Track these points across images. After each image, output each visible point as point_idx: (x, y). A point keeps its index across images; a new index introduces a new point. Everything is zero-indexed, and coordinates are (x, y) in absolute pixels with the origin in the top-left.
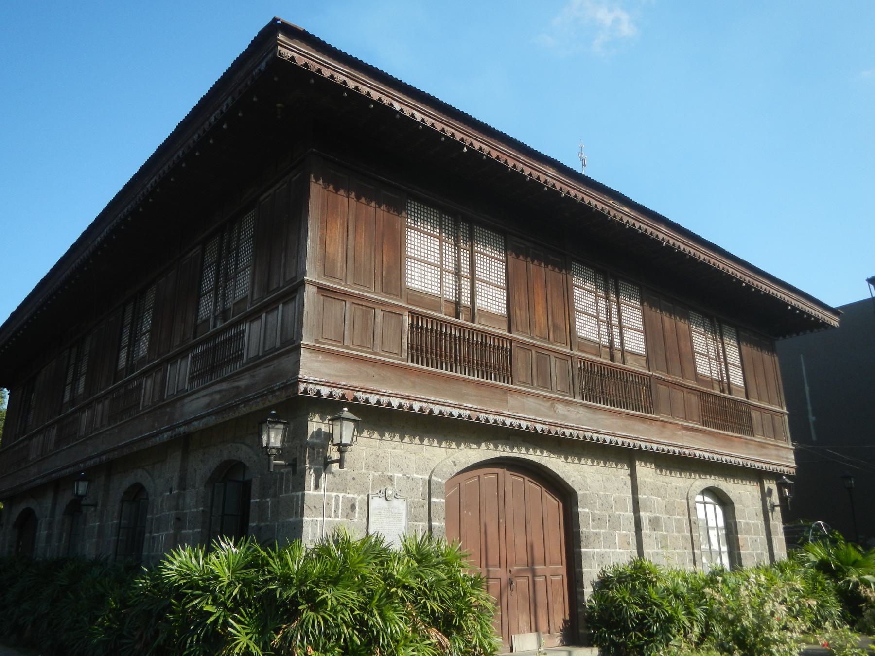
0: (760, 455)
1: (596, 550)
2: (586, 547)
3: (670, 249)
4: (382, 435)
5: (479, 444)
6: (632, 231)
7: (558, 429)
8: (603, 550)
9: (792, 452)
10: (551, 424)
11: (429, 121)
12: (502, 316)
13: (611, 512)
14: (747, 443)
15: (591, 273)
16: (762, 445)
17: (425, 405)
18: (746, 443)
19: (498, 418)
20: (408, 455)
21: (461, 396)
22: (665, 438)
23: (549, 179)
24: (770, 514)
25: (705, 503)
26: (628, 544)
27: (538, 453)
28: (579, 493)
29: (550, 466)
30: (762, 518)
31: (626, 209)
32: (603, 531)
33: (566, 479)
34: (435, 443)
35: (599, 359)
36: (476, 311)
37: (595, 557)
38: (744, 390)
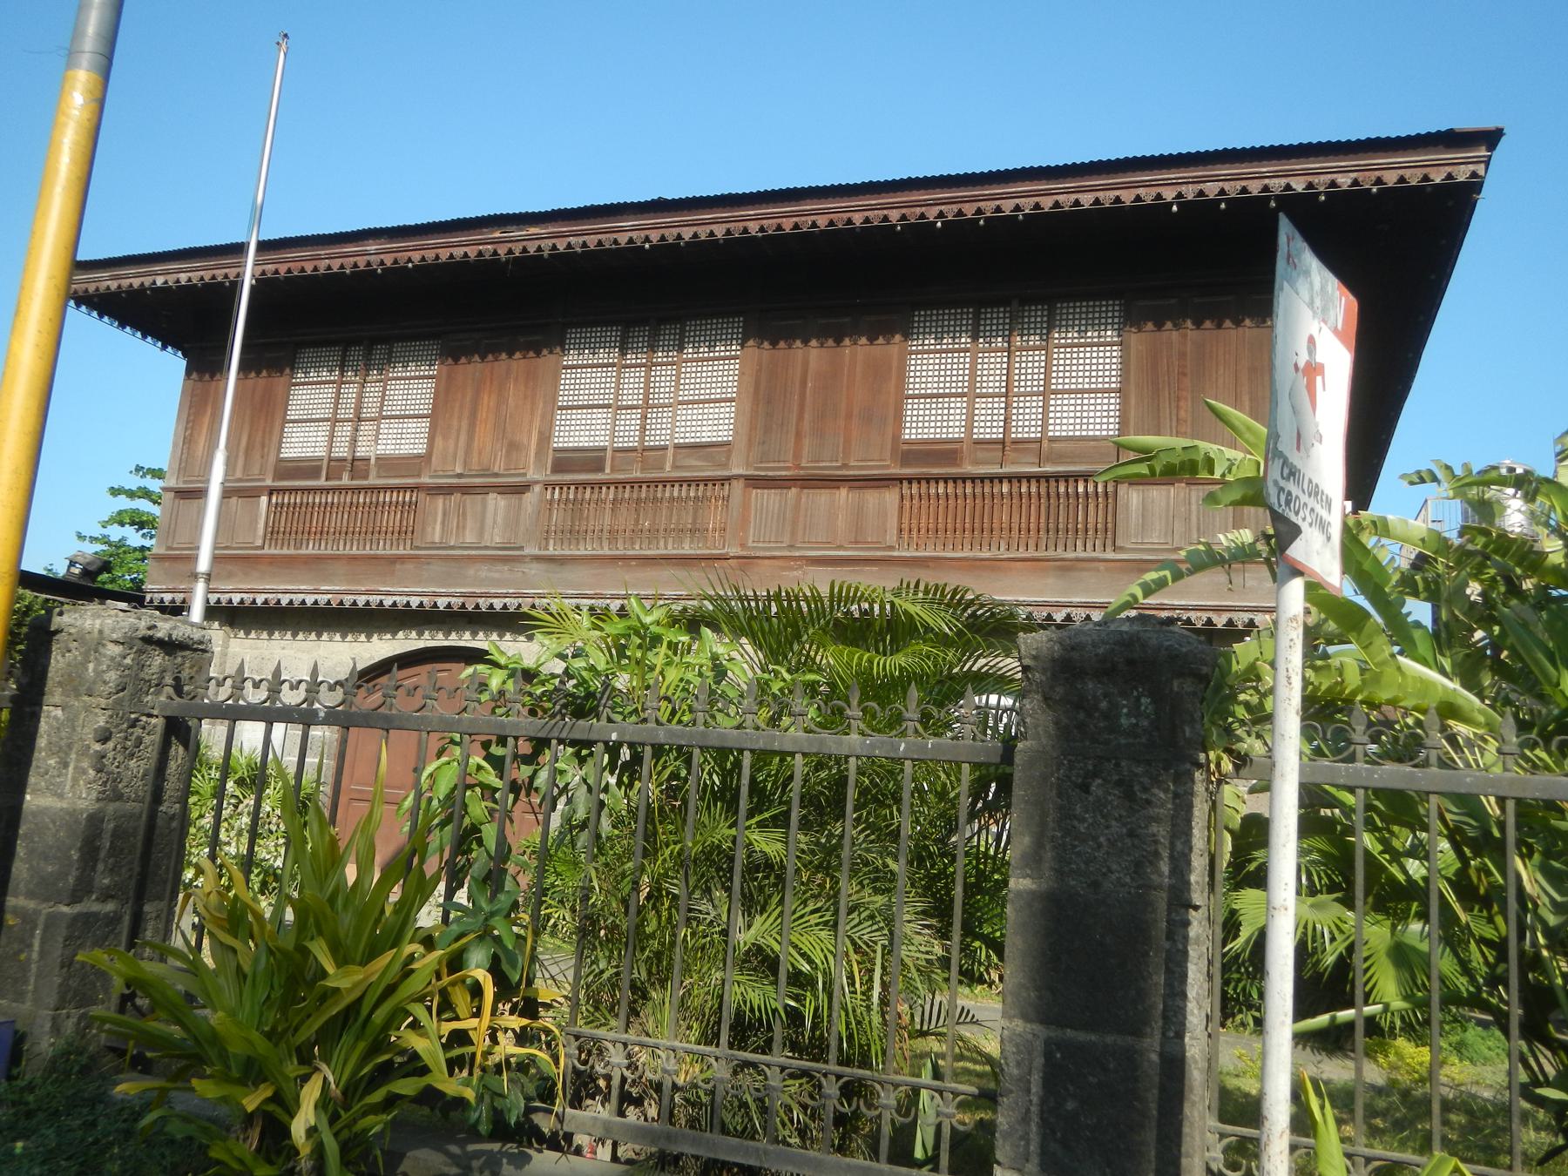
4: (271, 634)
5: (394, 634)
7: (481, 601)
10: (463, 595)
11: (195, 276)
12: (418, 456)
14: (1066, 568)
15: (615, 333)
17: (270, 596)
19: (371, 598)
20: (299, 655)
21: (326, 580)
23: (372, 258)
31: (533, 230)
34: (338, 637)
36: (373, 461)
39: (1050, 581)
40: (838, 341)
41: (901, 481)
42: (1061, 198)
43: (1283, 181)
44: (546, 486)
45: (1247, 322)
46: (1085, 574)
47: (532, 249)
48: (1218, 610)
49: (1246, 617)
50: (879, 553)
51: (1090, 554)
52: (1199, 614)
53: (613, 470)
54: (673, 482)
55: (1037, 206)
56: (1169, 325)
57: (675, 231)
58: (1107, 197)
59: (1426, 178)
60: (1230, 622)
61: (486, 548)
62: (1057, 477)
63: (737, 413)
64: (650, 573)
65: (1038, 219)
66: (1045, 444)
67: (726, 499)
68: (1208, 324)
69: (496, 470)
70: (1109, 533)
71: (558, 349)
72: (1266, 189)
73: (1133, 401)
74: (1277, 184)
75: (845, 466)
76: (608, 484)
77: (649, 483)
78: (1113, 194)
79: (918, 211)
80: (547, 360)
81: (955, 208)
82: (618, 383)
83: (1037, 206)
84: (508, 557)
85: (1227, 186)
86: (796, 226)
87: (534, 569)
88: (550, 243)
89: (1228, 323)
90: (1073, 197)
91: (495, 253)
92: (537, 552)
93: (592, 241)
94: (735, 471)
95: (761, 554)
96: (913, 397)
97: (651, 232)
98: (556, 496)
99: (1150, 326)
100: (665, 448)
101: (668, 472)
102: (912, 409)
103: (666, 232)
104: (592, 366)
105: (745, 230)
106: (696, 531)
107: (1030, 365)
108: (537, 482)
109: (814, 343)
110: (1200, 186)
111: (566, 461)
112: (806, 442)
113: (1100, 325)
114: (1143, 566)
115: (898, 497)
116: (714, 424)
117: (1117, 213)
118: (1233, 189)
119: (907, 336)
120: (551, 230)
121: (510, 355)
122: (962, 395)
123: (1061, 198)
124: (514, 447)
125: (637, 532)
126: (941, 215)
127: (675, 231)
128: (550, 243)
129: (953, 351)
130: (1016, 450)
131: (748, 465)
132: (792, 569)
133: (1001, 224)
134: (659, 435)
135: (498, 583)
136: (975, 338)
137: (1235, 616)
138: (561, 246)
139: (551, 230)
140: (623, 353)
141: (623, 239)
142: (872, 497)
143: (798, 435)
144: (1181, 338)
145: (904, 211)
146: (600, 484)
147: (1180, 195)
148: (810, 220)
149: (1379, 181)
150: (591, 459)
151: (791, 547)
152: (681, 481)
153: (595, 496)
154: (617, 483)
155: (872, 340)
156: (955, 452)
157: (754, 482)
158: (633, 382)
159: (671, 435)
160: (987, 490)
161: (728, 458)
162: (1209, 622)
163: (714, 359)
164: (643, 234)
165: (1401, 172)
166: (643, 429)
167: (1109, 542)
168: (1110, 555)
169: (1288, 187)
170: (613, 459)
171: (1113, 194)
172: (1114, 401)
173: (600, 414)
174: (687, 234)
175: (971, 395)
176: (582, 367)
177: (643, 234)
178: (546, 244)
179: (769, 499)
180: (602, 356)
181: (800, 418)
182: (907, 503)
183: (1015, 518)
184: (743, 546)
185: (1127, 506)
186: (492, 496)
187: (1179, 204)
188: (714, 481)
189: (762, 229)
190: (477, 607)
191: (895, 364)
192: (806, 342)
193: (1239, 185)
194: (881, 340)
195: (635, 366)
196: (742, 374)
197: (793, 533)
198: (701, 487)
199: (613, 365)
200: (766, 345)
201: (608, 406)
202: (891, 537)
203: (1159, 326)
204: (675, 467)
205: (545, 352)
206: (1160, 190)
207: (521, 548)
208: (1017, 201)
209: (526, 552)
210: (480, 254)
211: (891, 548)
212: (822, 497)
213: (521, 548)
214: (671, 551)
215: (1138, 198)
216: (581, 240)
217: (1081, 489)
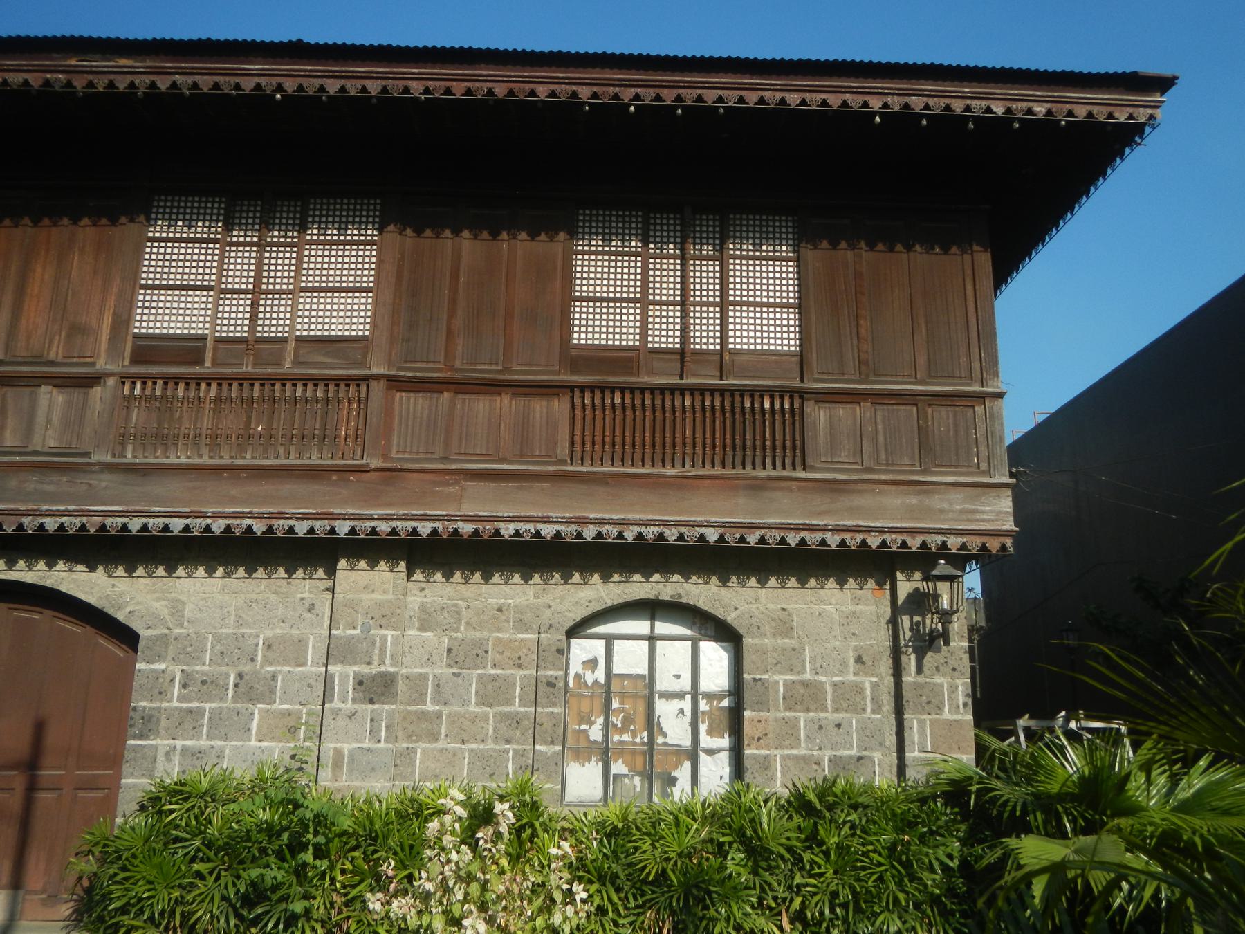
0: (821, 514)
1: (179, 744)
2: (141, 736)
3: (299, 101)
6: (153, 95)
7: (26, 521)
8: (203, 743)
9: (1009, 492)
13: (247, 668)
14: (757, 487)
16: (835, 487)
18: (752, 488)
22: (389, 505)
24: (910, 661)
25: (652, 639)
26: (293, 730)
27: (41, 565)
28: (143, 633)
29: (63, 588)
30: (886, 665)
31: (123, 62)
32: (207, 706)
33: (110, 611)
35: (197, 370)
37: (176, 759)
38: (797, 359)
39: (741, 500)
40: (495, 235)
41: (572, 389)
42: (766, 95)
43: (984, 104)
44: (123, 379)
45: (918, 248)
46: (779, 494)
47: (122, 84)
48: (913, 532)
49: (939, 539)
50: (551, 468)
51: (779, 473)
52: (894, 536)
53: (214, 364)
54: (294, 380)
55: (741, 100)
56: (843, 245)
57: (317, 82)
58: (814, 99)
59: (1110, 116)
60: (924, 545)
61: (36, 453)
62: (742, 391)
63: (375, 304)
64: (266, 487)
65: (740, 114)
66: (727, 357)
67: (363, 403)
68: (880, 246)
69: (52, 356)
70: (798, 453)
71: (142, 218)
72: (968, 109)
73: (813, 317)
74: (979, 106)
75: (506, 370)
76: (209, 380)
77: (263, 380)
78: (820, 97)
79: (611, 90)
80: (127, 229)
81: (653, 92)
82: (221, 263)
83: (741, 100)
84: (67, 464)
85: (931, 102)
86: (469, 92)
87: (105, 481)
88: (147, 79)
89: (899, 247)
90: (779, 95)
91: (69, 84)
92: (109, 459)
93: (206, 83)
94: (375, 370)
95: (410, 466)
96: (581, 299)
97: (290, 80)
98: (138, 391)
99: (825, 244)
100: (284, 341)
101: (287, 366)
102: (579, 312)
103: (306, 82)
104: (187, 240)
105: (406, 90)
106: (326, 438)
107: (705, 276)
108: (111, 374)
109: (466, 234)
110: (906, 99)
111: (152, 350)
112: (460, 342)
113: (774, 239)
114: (837, 486)
115: (569, 406)
116: (348, 317)
117: (823, 116)
118: (937, 105)
119: (572, 234)
120: (149, 63)
121: (75, 220)
122: (635, 301)
123: (766, 95)
124: (77, 330)
125: (246, 438)
126: (637, 97)
127: (317, 82)
128: (147, 79)
129: (623, 254)
130: (693, 362)
131: (390, 364)
132: (447, 484)
133: (700, 115)
134: (275, 323)
135: (54, 498)
136: (646, 243)
137: (929, 539)
138: (163, 84)
139: (149, 63)
140: (228, 228)
141: (248, 84)
142: (538, 407)
143: (450, 333)
144: (858, 259)
145: (595, 89)
146: (198, 380)
147: (886, 106)
148: (485, 87)
149: (1070, 114)
150: (187, 349)
151: (445, 459)
152: (305, 380)
153: (192, 393)
154: (220, 380)
155: (533, 235)
156: (630, 360)
157: (395, 383)
158: (240, 266)
159: (292, 326)
160: (668, 402)
161: (365, 356)
162: (904, 544)
163: (345, 243)
164: (275, 81)
165: (1089, 108)
166: (254, 317)
167: (798, 460)
168: (803, 475)
169: (989, 110)
170: (215, 350)
171: (820, 97)
172: (791, 319)
173: (199, 297)
174: (333, 87)
175: (644, 302)
176: (174, 240)
177: (275, 81)
178: (142, 81)
179: (414, 404)
180: (201, 230)
181: (452, 314)
182: (578, 412)
183: (699, 435)
184: (386, 456)
185: (814, 422)
186: (44, 389)
187: (882, 115)
188: (348, 380)
189: (427, 91)
190: (20, 527)
191: (560, 263)
192: (457, 232)
193: (943, 102)
194: (543, 237)
195: (244, 244)
196: (380, 262)
197: (447, 443)
198: (332, 388)
199: (215, 241)
200: (409, 231)
201: (209, 288)
202: (563, 451)
203: (834, 245)
204: (297, 362)
205: (123, 220)
206: (867, 98)
207: (87, 454)
208: (720, 92)
209: (95, 458)
210: (47, 83)
211: (563, 462)
212: (482, 405)
213: (87, 454)
214: (293, 461)
215: (845, 104)
216: (190, 80)
217: (767, 405)
